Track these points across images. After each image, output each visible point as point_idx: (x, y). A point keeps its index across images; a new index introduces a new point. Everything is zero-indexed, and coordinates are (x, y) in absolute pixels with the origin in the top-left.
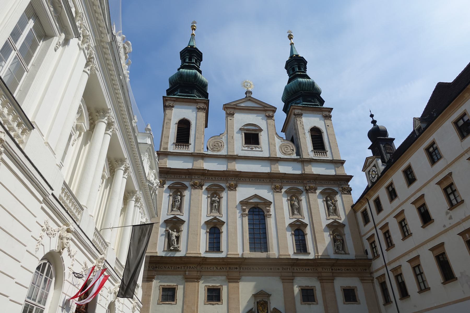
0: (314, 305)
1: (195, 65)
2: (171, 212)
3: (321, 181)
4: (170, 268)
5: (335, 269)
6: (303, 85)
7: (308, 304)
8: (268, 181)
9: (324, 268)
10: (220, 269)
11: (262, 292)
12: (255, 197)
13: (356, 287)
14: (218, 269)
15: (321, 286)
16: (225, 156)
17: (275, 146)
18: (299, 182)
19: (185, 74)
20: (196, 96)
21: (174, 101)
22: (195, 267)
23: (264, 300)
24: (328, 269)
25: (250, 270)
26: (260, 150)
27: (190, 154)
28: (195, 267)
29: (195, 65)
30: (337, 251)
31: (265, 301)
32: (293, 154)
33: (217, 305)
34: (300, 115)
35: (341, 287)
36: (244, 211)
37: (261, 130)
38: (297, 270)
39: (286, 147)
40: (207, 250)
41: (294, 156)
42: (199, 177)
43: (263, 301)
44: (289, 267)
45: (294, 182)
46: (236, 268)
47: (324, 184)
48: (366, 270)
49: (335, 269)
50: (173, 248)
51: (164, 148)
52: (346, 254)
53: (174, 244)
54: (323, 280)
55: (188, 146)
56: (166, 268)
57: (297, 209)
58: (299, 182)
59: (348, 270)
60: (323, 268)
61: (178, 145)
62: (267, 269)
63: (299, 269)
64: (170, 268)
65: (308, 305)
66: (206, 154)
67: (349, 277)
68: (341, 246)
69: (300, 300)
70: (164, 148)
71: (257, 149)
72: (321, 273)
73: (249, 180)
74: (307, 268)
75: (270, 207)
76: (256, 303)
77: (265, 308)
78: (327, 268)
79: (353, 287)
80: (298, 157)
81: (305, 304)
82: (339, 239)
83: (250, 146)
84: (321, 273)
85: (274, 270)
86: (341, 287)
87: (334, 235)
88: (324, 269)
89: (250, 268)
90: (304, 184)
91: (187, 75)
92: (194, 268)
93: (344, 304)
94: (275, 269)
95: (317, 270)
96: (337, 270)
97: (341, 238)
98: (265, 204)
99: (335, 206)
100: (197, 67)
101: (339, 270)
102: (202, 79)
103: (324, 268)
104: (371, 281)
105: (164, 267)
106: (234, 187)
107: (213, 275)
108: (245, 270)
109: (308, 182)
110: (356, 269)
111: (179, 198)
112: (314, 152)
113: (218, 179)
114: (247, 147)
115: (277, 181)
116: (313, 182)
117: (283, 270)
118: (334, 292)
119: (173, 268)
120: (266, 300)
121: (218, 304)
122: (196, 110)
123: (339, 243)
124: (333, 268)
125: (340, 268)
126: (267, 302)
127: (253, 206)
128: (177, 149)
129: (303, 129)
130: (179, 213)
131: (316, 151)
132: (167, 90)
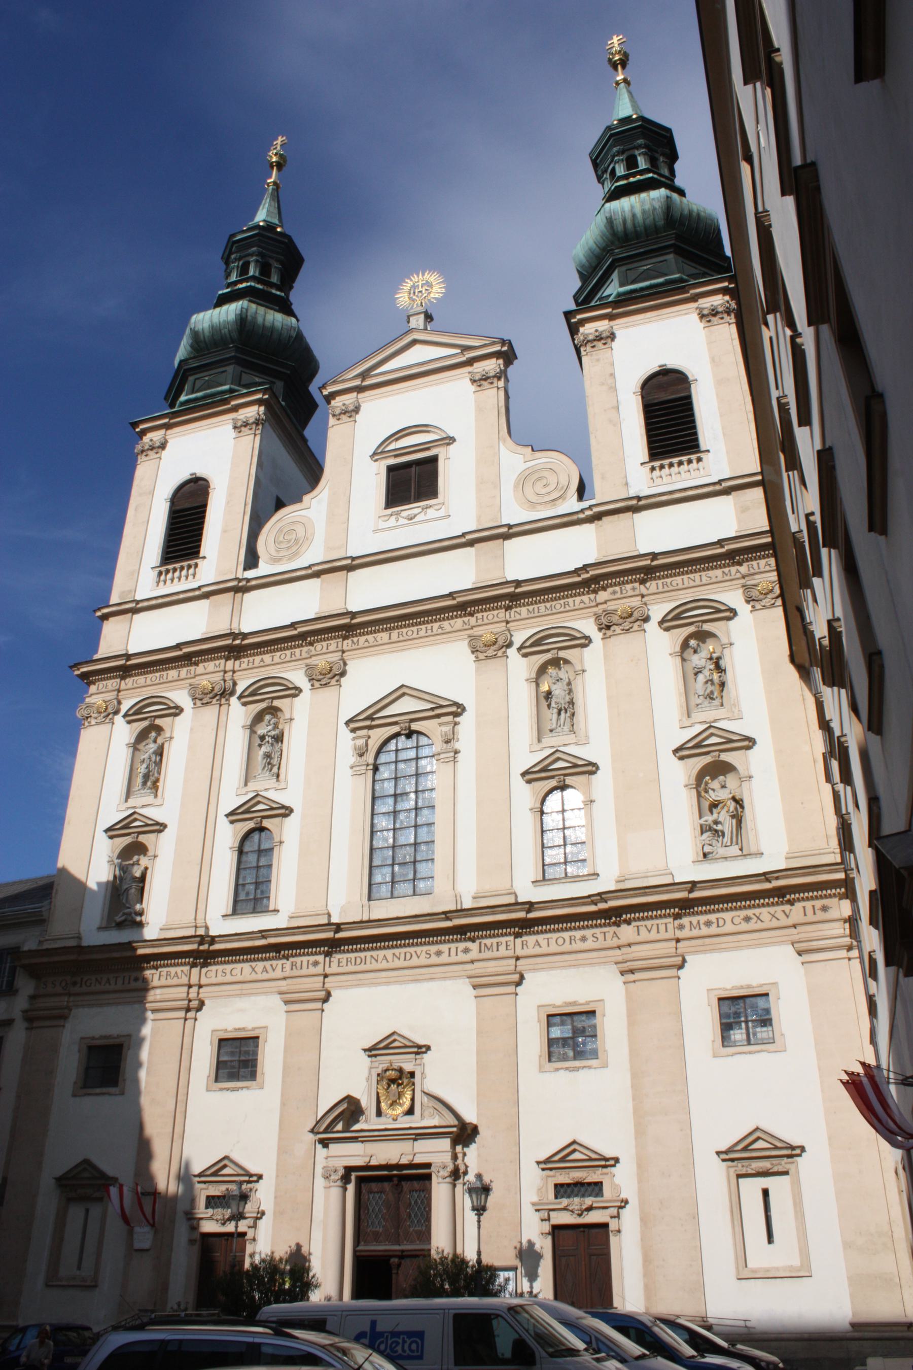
0: (592, 1070)
1: (253, 284)
2: (126, 801)
3: (669, 580)
4: (113, 982)
5: (691, 922)
6: (624, 221)
7: (567, 1069)
8: (458, 623)
9: (646, 926)
10: (265, 970)
11: (395, 1040)
12: (404, 694)
13: (775, 984)
14: (256, 973)
15: (629, 998)
16: (310, 571)
17: (497, 485)
18: (577, 602)
19: (206, 325)
20: (237, 388)
21: (168, 427)
22: (182, 971)
23: (396, 1066)
24: (662, 928)
25: (365, 963)
26: (442, 513)
27: (197, 593)
28: (182, 971)
29: (253, 284)
30: (707, 849)
31: (400, 1070)
32: (565, 499)
33: (245, 1092)
34: (601, 339)
35: (708, 990)
36: (361, 755)
37: (450, 440)
38: (537, 947)
39: (539, 479)
40: (230, 911)
41: (572, 504)
42: (217, 664)
43: (395, 1070)
44: (503, 940)
45: (558, 606)
46: (316, 963)
47: (680, 586)
48: (825, 909)
49: (691, 922)
50: (123, 918)
51: (122, 594)
52: (744, 855)
53: (127, 905)
54: (632, 972)
55: (196, 565)
56: (100, 983)
57: (563, 713)
58: (577, 602)
59: (747, 919)
60: (638, 927)
61: (168, 571)
62: (424, 952)
63: (543, 943)
64: (113, 982)
65: (567, 1071)
66: (248, 580)
67: (748, 947)
68: (728, 825)
69: (537, 1058)
70: (123, 592)
71: (431, 513)
72: (629, 945)
73: (390, 638)
74: (578, 934)
75: (456, 724)
76: (375, 1078)
77: (400, 1095)
78: (658, 925)
79: (761, 985)
80: (585, 504)
81: (557, 1070)
82: (719, 802)
83: (402, 511)
84: (629, 945)
85: (449, 955)
86: (708, 990)
87: (703, 786)
88: (643, 931)
89: (366, 957)
90: (597, 605)
91: (213, 326)
92: (180, 976)
93: (715, 1056)
94: (453, 951)
95: (617, 936)
96: (702, 926)
97: (731, 796)
98: (438, 716)
99: (719, 668)
100: (260, 286)
101: (708, 924)
102: (268, 324)
103: (646, 926)
104: (843, 953)
105: (97, 979)
106: (329, 676)
107: (238, 992)
108: (347, 965)
109: (614, 593)
110: (783, 911)
111: (152, 751)
112: (653, 469)
113: (283, 657)
114: (392, 515)
115: (490, 617)
116: (634, 589)
117: (480, 952)
118: (678, 1014)
119: (120, 981)
120: (408, 1067)
121: (248, 1088)
122: (232, 433)
123: (724, 812)
124: (685, 921)
125: (712, 917)
126: (412, 1074)
127: (396, 729)
128: (162, 583)
129: (613, 388)
130: (150, 799)
131: (657, 464)
132: (166, 398)
